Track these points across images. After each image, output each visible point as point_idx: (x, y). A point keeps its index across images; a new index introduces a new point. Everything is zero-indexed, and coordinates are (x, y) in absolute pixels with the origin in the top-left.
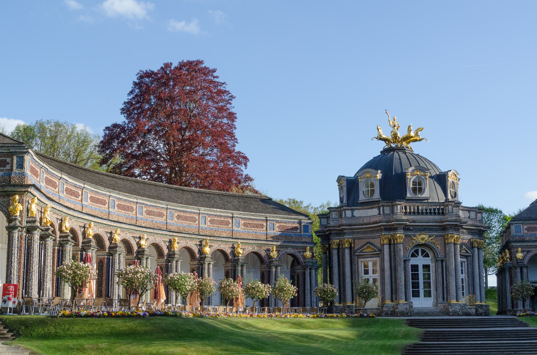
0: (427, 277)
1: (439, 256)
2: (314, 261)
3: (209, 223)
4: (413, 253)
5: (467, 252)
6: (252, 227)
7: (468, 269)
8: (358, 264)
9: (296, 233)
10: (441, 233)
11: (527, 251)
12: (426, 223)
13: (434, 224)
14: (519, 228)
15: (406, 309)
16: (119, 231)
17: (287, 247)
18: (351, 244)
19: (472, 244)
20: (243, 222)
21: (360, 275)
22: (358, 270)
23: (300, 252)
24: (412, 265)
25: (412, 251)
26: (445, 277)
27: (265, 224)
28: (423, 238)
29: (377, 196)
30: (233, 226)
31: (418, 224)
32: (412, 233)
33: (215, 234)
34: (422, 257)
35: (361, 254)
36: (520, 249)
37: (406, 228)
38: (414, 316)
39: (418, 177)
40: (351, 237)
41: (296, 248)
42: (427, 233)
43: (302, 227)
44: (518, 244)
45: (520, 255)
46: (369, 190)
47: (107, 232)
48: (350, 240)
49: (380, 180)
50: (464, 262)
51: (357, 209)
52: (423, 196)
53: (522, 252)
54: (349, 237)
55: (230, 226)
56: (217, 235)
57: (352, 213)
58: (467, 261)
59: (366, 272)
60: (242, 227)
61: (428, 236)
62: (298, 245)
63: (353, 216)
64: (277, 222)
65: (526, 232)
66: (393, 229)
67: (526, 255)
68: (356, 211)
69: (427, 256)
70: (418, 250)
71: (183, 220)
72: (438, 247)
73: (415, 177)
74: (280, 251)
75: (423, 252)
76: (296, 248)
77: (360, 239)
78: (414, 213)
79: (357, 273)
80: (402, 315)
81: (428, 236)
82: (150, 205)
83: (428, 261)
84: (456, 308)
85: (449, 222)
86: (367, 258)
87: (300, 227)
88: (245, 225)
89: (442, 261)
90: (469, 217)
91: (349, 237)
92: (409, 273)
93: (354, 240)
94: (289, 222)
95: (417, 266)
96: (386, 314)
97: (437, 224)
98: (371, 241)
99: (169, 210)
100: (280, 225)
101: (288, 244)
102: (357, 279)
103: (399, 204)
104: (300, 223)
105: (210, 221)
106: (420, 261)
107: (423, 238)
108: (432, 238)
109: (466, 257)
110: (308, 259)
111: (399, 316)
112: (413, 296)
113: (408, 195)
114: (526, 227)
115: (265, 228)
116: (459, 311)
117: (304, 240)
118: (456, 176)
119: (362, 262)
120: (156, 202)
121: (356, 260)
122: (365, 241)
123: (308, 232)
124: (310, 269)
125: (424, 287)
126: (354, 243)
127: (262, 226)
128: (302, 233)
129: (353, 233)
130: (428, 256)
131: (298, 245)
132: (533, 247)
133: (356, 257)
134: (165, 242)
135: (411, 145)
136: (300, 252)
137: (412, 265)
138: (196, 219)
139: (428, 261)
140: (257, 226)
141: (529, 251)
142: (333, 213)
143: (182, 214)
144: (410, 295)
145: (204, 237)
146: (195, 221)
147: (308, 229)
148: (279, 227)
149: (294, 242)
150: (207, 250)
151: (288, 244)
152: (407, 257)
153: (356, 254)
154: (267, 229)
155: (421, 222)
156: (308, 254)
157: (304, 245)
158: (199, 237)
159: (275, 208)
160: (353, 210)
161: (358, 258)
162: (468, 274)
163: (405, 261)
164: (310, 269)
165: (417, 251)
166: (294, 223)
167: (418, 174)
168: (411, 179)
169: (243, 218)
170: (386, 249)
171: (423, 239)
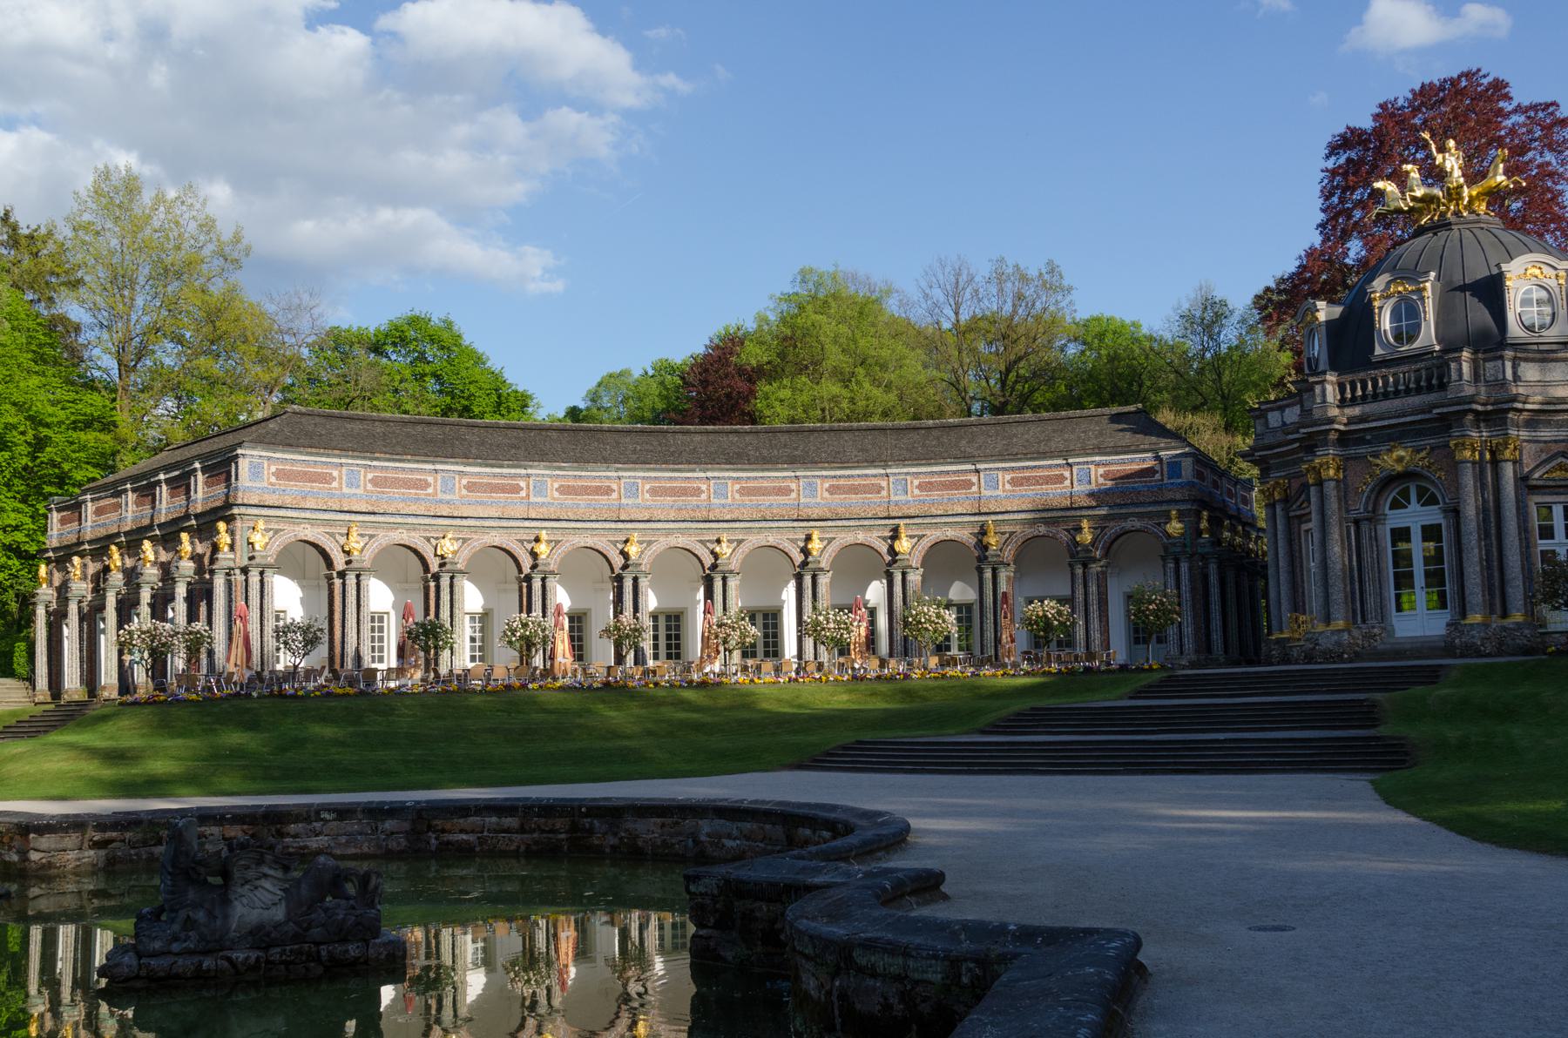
2: (1202, 541)
3: (917, 492)
4: (1394, 498)
9: (1150, 482)
12: (1398, 417)
15: (1339, 644)
16: (635, 537)
17: (1125, 517)
18: (1286, 490)
20: (1008, 477)
22: (1301, 551)
23: (1159, 524)
24: (1393, 530)
27: (1067, 474)
28: (1396, 458)
30: (982, 489)
32: (1370, 450)
33: (935, 512)
35: (1298, 513)
37: (1344, 439)
38: (1363, 660)
39: (1403, 298)
40: (1283, 474)
41: (1149, 515)
42: (1409, 444)
47: (614, 543)
49: (1328, 323)
51: (1288, 406)
52: (1414, 346)
55: (975, 489)
56: (939, 512)
60: (1008, 487)
61: (1410, 449)
62: (1150, 509)
63: (1284, 424)
64: (1098, 464)
66: (1311, 444)
68: (1287, 410)
69: (1432, 501)
70: (1408, 487)
71: (845, 493)
72: (1439, 478)
73: (1392, 301)
74: (1105, 527)
76: (1149, 515)
78: (1375, 397)
80: (1327, 661)
81: (1410, 449)
82: (749, 478)
83: (1433, 515)
84: (1473, 637)
85: (1443, 406)
87: (1162, 469)
88: (1013, 482)
93: (1289, 481)
94: (1132, 461)
96: (1305, 657)
99: (801, 481)
101: (1123, 511)
102: (1299, 574)
103: (1317, 383)
104: (1158, 458)
105: (920, 487)
106: (1415, 516)
107: (1396, 458)
108: (1423, 454)
110: (1175, 538)
111: (1320, 663)
113: (1378, 351)
115: (1067, 483)
116: (1482, 645)
117: (1170, 495)
118: (1555, 269)
120: (763, 470)
123: (1180, 476)
124: (1177, 562)
126: (1289, 487)
127: (1061, 479)
128: (1165, 482)
130: (1438, 503)
131: (1150, 509)
133: (1296, 521)
134: (794, 541)
136: (1159, 524)
137: (1393, 530)
138: (883, 488)
139: (1433, 515)
140: (1048, 480)
143: (842, 482)
144: (1382, 607)
145: (896, 521)
146: (879, 492)
147: (1180, 469)
148: (1105, 476)
149: (1142, 504)
150: (903, 545)
151: (1123, 511)
152: (1362, 511)
153: (1292, 514)
154: (1072, 484)
155: (1383, 419)
156: (1175, 527)
157: (1164, 508)
158: (891, 522)
159: (1121, 430)
161: (1301, 523)
163: (1357, 522)
164: (1177, 562)
165: (1405, 494)
166: (1144, 460)
167: (1399, 292)
168: (1381, 308)
169: (1004, 469)
171: (1400, 460)
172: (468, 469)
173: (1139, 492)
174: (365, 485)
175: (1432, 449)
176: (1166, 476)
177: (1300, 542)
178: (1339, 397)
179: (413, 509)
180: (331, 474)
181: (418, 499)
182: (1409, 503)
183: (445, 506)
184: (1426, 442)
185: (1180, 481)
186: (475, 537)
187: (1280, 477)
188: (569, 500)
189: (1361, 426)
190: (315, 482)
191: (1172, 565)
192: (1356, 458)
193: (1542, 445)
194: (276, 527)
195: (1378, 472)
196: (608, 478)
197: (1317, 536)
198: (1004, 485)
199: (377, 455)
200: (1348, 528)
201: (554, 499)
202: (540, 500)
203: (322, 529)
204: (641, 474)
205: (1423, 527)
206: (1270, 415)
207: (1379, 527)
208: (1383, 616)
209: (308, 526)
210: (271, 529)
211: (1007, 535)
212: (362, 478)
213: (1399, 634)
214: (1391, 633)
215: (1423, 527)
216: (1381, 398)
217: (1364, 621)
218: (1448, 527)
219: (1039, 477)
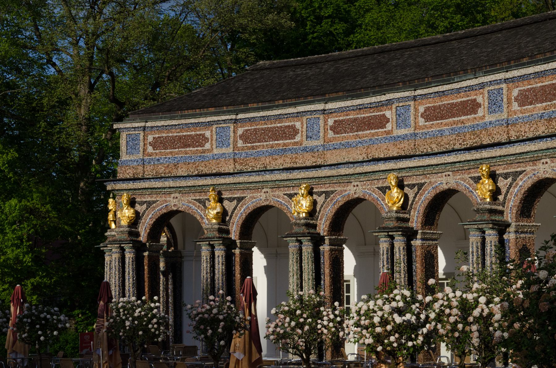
172: (330, 106)
174: (235, 142)
179: (280, 163)
180: (203, 135)
181: (285, 150)
183: (308, 156)
186: (339, 189)
188: (435, 126)
190: (189, 146)
194: (149, 199)
196: (470, 88)
199: (250, 106)
201: (421, 128)
202: (403, 132)
203: (191, 197)
204: (501, 76)
209: (177, 195)
210: (234, 198)
212: (232, 134)
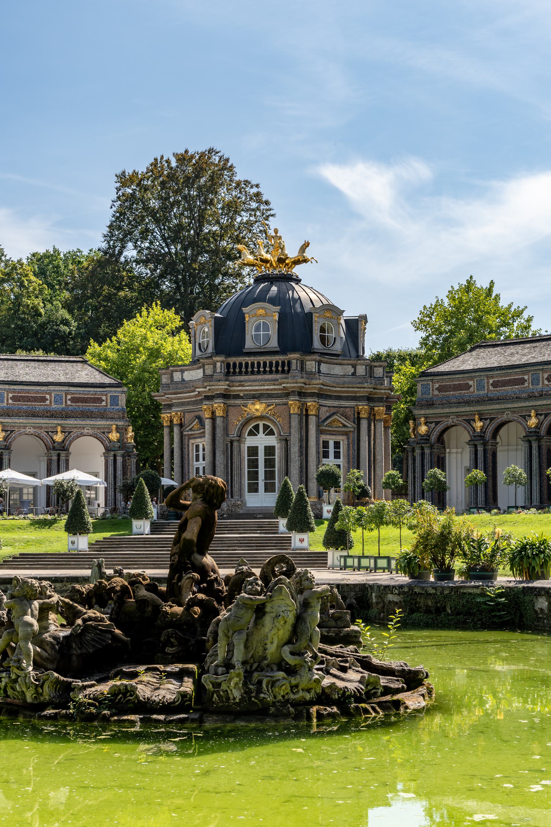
0: (269, 463)
1: (282, 434)
5: (344, 426)
6: (27, 402)
7: (348, 450)
8: (188, 448)
9: (99, 406)
10: (284, 400)
11: (435, 422)
13: (272, 387)
14: (427, 387)
18: (181, 420)
19: (359, 413)
20: (11, 395)
21: (191, 462)
22: (188, 455)
23: (104, 433)
24: (248, 447)
25: (250, 427)
26: (229, 464)
29: (210, 350)
31: (247, 388)
34: (263, 436)
35: (190, 433)
36: (422, 419)
40: (180, 409)
42: (264, 401)
43: (109, 398)
44: (422, 412)
45: (423, 429)
46: (328, 333)
48: (179, 413)
50: (343, 440)
51: (187, 370)
53: (426, 424)
54: (177, 409)
57: (182, 376)
58: (348, 439)
59: (197, 460)
60: (10, 401)
63: (183, 380)
65: (436, 393)
67: (434, 428)
68: (186, 373)
69: (271, 433)
70: (258, 425)
74: (71, 432)
75: (266, 427)
77: (190, 412)
79: (187, 460)
83: (272, 441)
86: (197, 438)
88: (13, 398)
89: (286, 441)
90: (354, 374)
91: (177, 409)
92: (280, 457)
95: (257, 447)
97: (276, 387)
98: (200, 413)
100: (74, 397)
107: (258, 408)
108: (271, 407)
109: (346, 434)
112: (249, 491)
114: (437, 385)
119: (193, 444)
121: (186, 442)
122: (193, 414)
123: (117, 405)
125: (266, 478)
126: (184, 417)
128: (109, 406)
129: (182, 404)
130: (274, 435)
132: (444, 416)
135: (297, 270)
136: (104, 433)
137: (248, 447)
139: (272, 441)
140: (36, 399)
141: (439, 422)
142: (163, 376)
144: (241, 489)
152: (235, 435)
153: (185, 433)
160: (182, 372)
161: (190, 439)
162: (349, 459)
165: (257, 427)
170: (208, 424)
173: (92, 412)
175: (276, 405)
176: (109, 404)
177: (188, 450)
178: (226, 370)
182: (259, 433)
184: (273, 401)
185: (117, 407)
187: (179, 411)
189: (240, 388)
191: (112, 458)
192: (234, 406)
193: (327, 408)
195: (246, 415)
197: (208, 448)
198: (8, 400)
200: (227, 445)
205: (266, 448)
206: (175, 374)
207: (242, 445)
208: (241, 495)
211: (9, 432)
213: (248, 505)
214: (244, 503)
215: (266, 448)
216: (243, 374)
217: (232, 497)
218: (281, 448)
219: (31, 396)
